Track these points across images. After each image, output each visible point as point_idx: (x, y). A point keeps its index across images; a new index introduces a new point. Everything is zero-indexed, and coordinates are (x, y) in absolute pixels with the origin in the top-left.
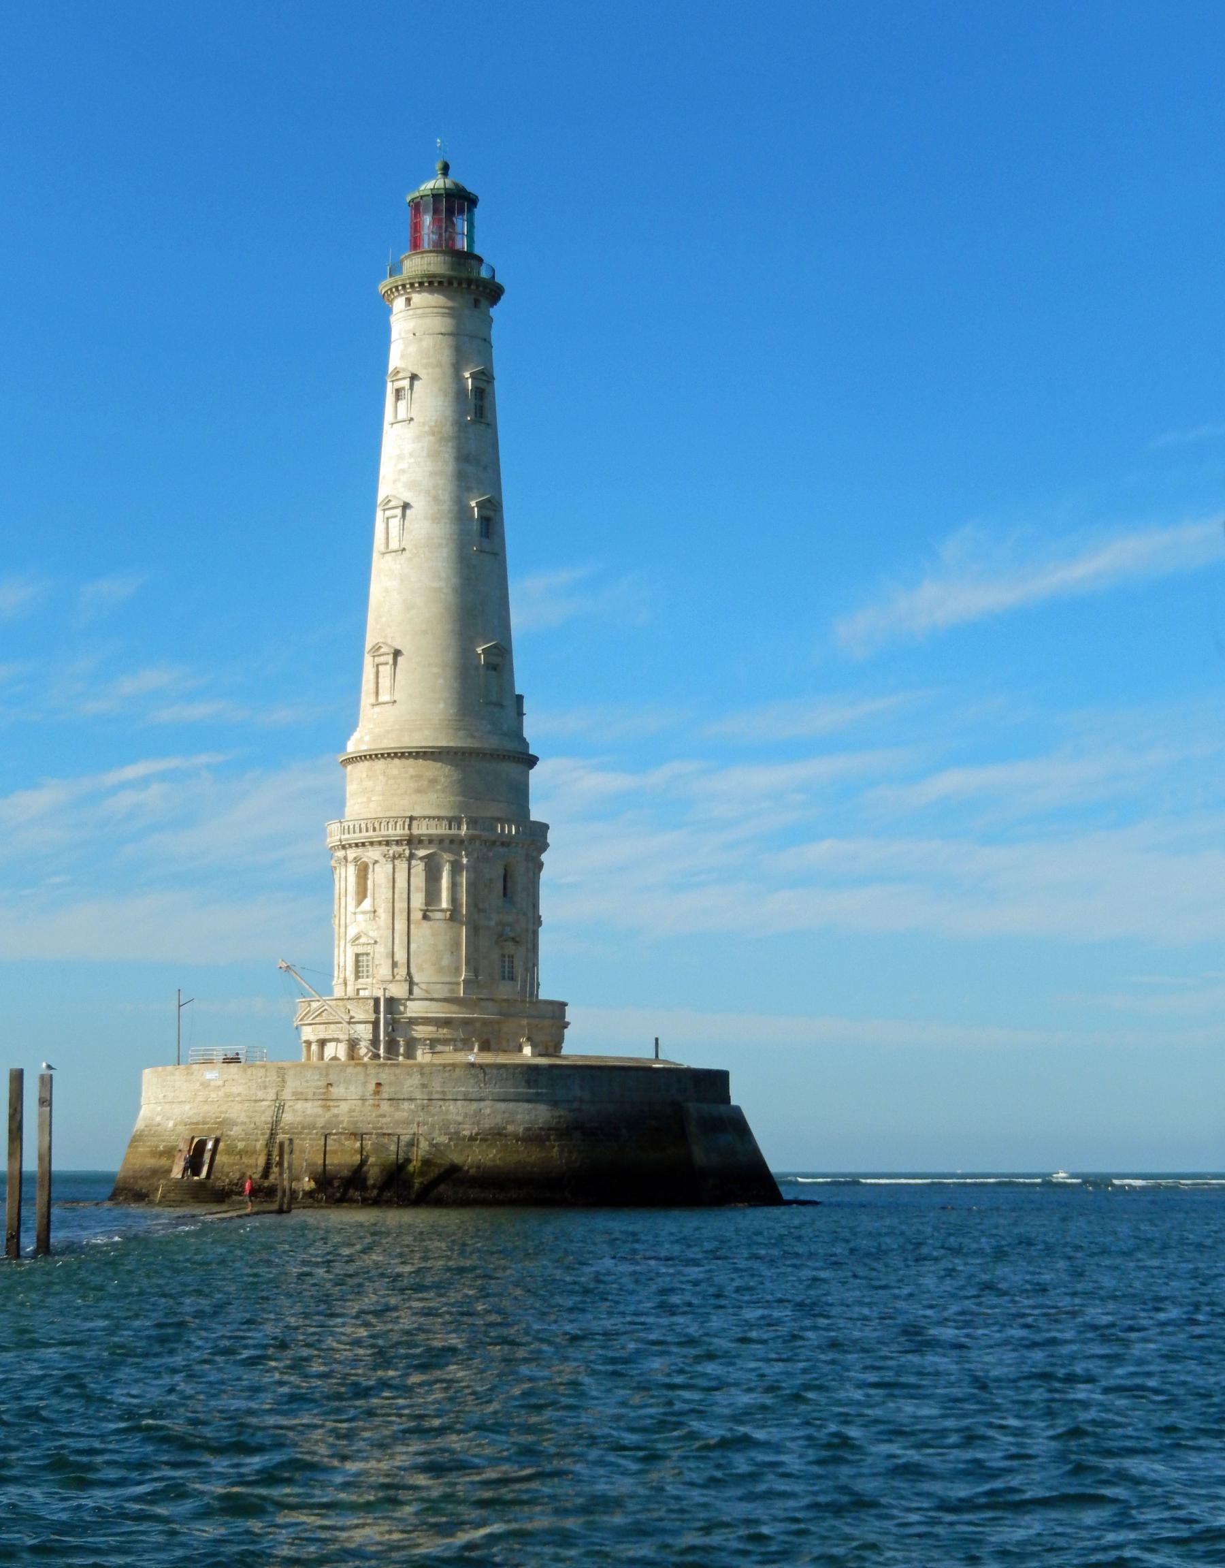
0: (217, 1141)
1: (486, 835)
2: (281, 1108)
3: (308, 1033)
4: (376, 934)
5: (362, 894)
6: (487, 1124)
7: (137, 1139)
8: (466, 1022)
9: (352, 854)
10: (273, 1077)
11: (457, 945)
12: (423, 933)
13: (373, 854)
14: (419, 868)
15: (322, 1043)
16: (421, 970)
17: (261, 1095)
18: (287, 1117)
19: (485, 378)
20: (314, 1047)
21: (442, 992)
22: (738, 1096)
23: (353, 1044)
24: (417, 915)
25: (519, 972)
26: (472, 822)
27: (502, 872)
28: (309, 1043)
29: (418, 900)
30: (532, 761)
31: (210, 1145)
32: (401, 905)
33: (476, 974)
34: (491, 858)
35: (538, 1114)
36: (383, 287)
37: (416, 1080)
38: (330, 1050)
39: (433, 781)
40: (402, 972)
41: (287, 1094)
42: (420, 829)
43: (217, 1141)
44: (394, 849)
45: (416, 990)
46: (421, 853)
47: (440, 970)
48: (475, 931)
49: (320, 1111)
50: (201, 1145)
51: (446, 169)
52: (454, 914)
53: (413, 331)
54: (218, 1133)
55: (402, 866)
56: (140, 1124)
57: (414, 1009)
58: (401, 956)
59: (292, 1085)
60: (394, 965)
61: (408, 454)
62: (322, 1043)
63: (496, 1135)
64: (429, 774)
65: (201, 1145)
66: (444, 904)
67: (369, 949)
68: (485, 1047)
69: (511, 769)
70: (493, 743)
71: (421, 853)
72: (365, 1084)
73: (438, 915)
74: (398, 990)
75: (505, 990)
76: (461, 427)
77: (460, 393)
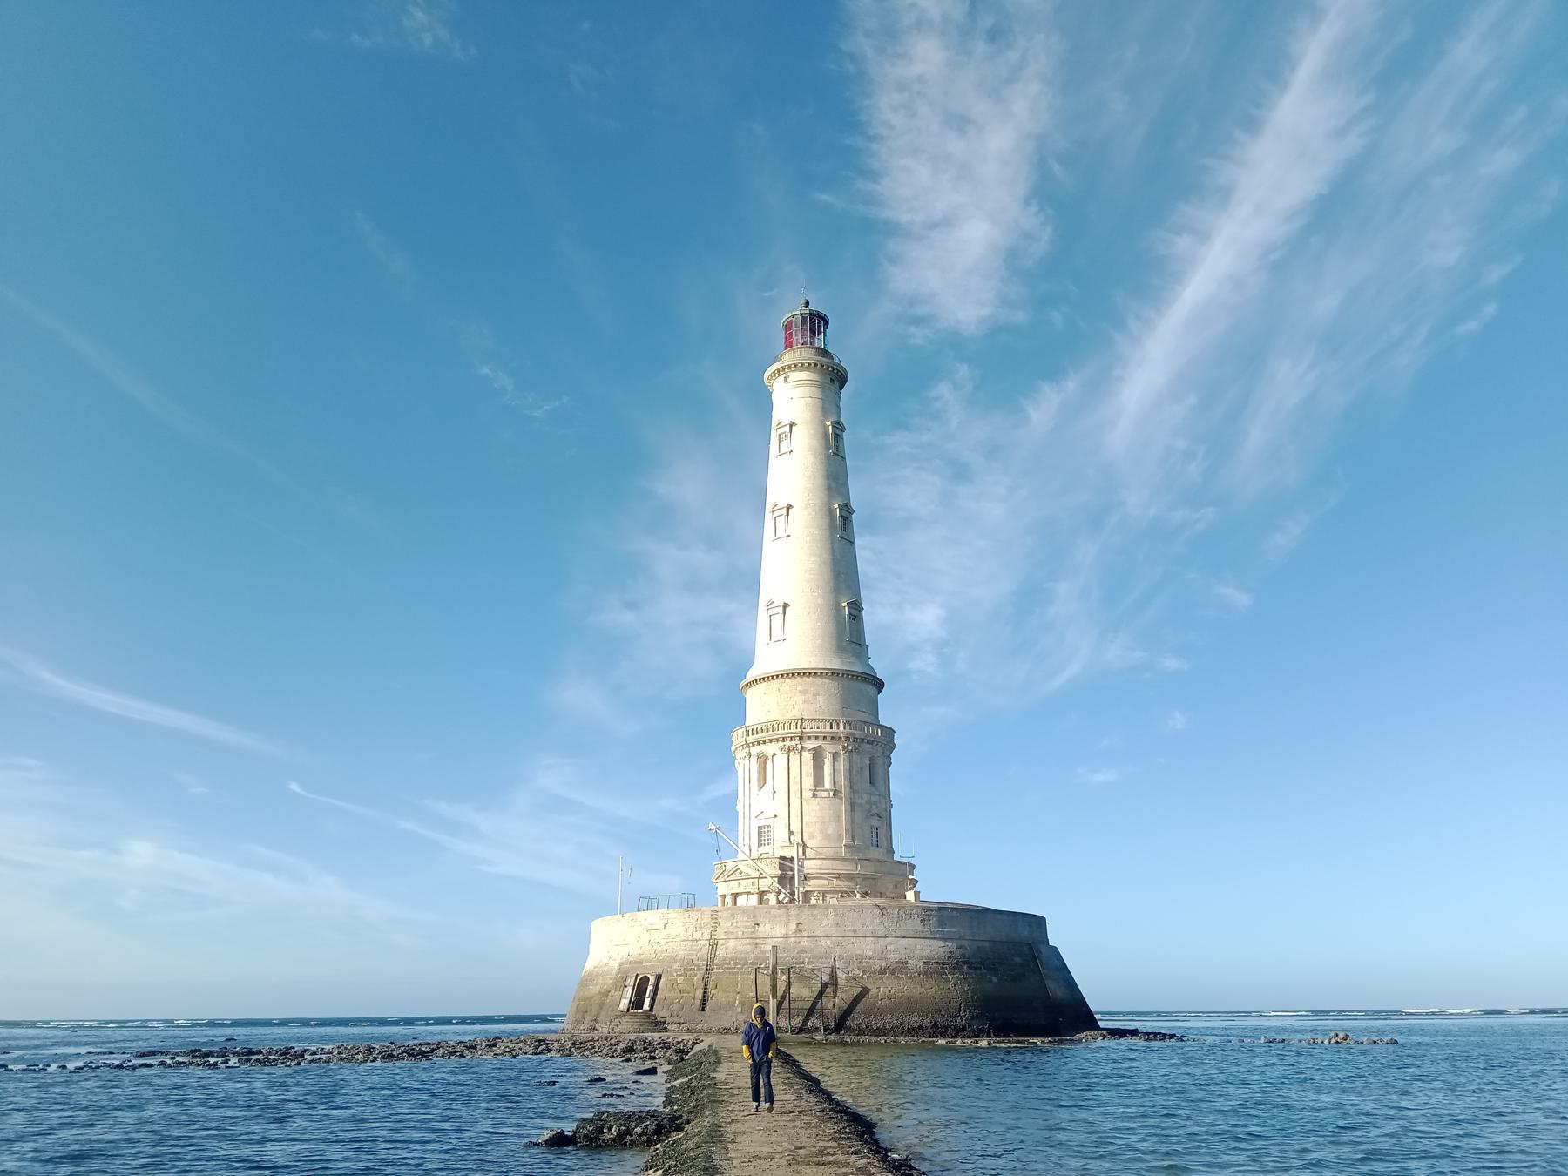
0: (659, 977)
1: (858, 733)
2: (714, 945)
3: (722, 889)
4: (780, 806)
5: (762, 781)
6: (893, 957)
7: (587, 981)
8: (850, 877)
9: (755, 750)
10: (707, 919)
11: (839, 817)
12: (813, 808)
13: (769, 749)
14: (807, 756)
15: (735, 896)
16: (812, 837)
17: (697, 935)
18: (720, 953)
19: (839, 428)
20: (728, 900)
21: (829, 852)
22: (1055, 937)
23: (762, 894)
24: (807, 794)
25: (883, 842)
26: (848, 724)
27: (867, 762)
28: (724, 896)
29: (808, 782)
30: (880, 685)
31: (652, 981)
32: (795, 787)
33: (853, 839)
34: (863, 751)
35: (934, 948)
36: (766, 375)
37: (830, 919)
38: (741, 901)
39: (816, 694)
40: (797, 838)
41: (720, 934)
42: (809, 729)
43: (659, 977)
44: (788, 743)
45: (809, 853)
46: (810, 745)
47: (827, 837)
48: (852, 805)
49: (749, 948)
50: (645, 980)
51: (807, 304)
52: (836, 792)
53: (792, 397)
54: (659, 971)
55: (795, 757)
56: (589, 966)
57: (810, 866)
58: (796, 827)
59: (724, 924)
60: (791, 833)
61: (792, 472)
62: (735, 896)
63: (899, 969)
64: (812, 689)
65: (645, 980)
66: (828, 784)
67: (769, 822)
68: (865, 894)
69: (872, 690)
70: (858, 668)
71: (810, 745)
72: (787, 923)
73: (824, 794)
74: (791, 852)
75: (876, 853)
76: (828, 458)
77: (826, 435)
